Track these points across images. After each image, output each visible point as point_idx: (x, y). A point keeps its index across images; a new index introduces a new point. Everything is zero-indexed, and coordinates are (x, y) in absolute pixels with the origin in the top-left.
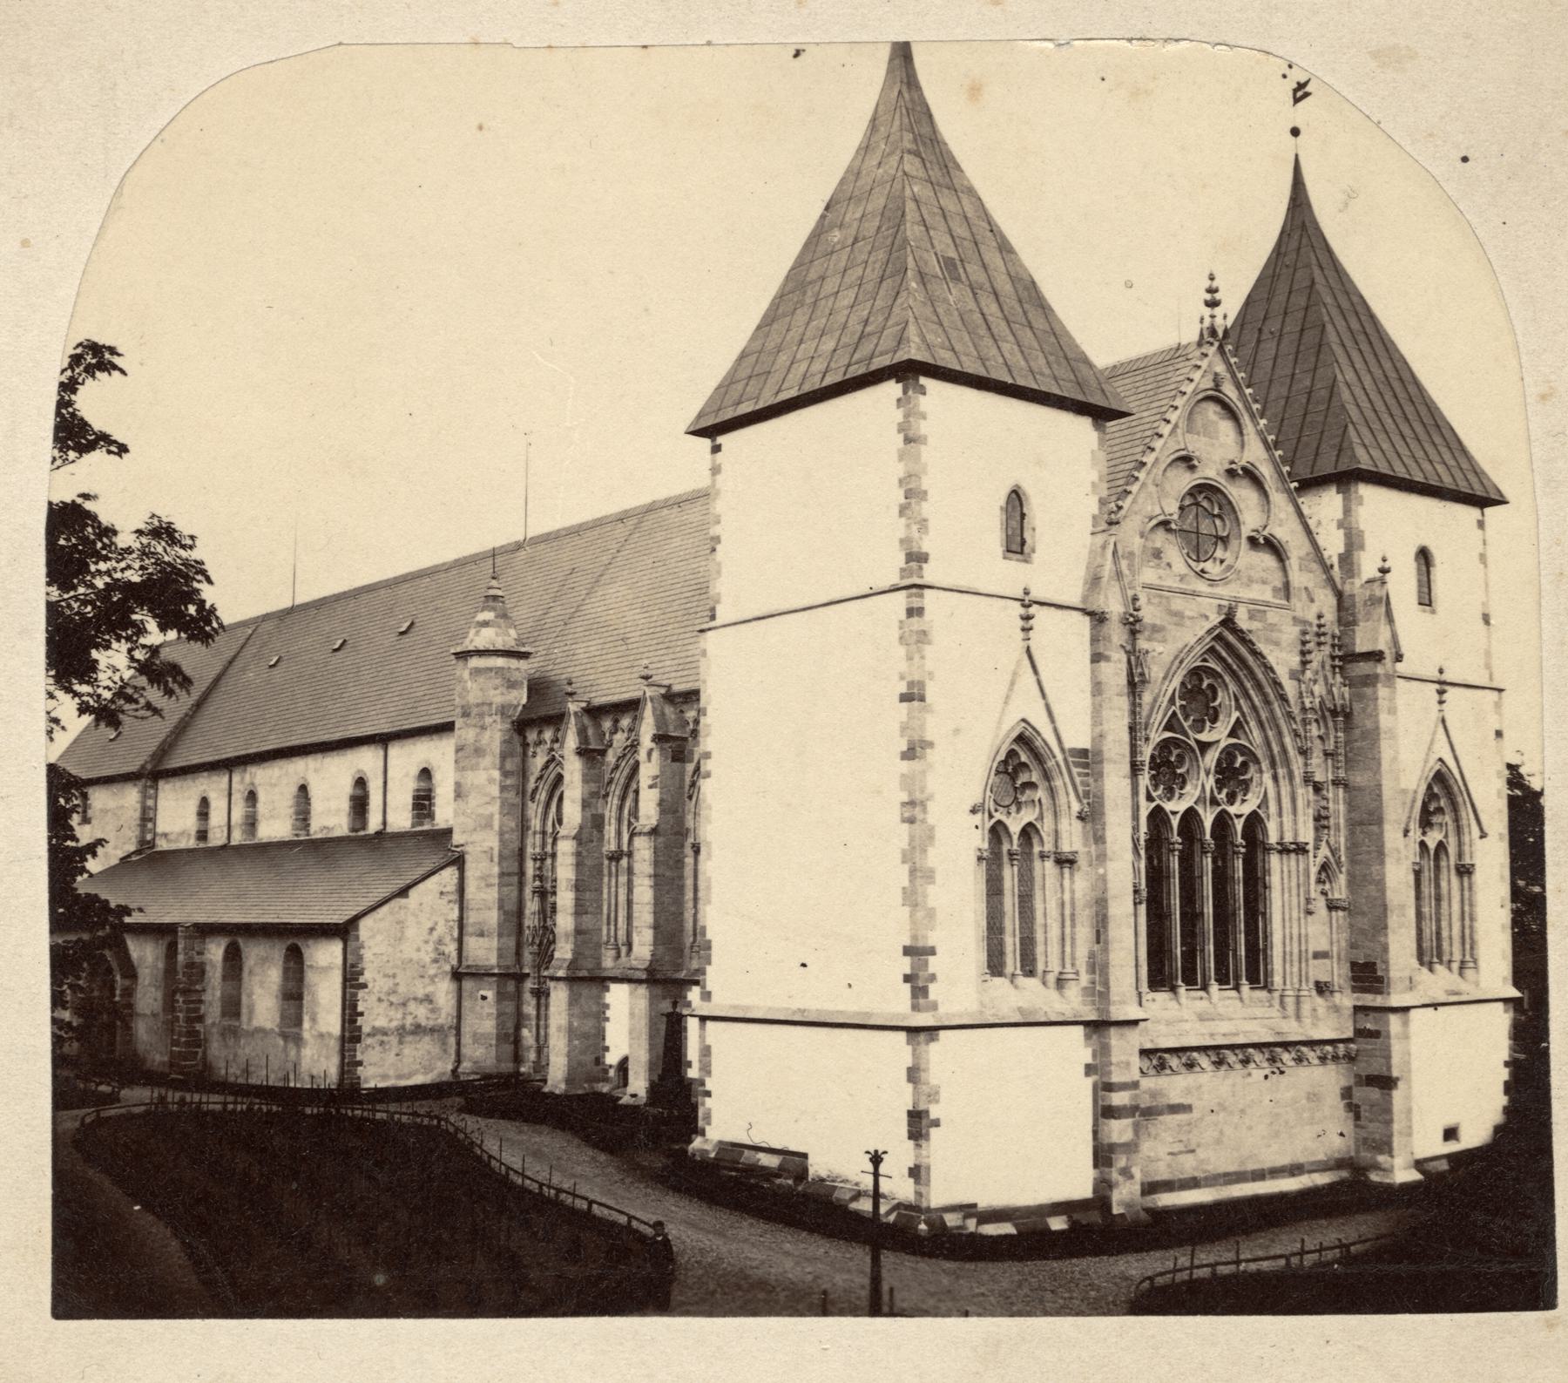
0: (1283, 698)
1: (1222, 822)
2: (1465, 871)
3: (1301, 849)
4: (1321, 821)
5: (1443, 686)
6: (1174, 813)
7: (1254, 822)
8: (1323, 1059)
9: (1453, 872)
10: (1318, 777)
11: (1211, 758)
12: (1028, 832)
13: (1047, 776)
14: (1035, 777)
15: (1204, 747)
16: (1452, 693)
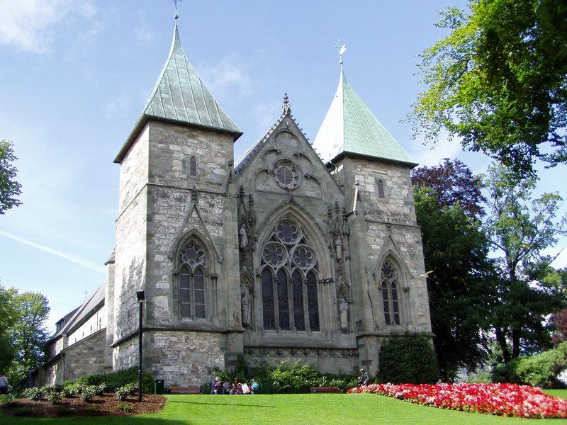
0: (320, 229)
1: (297, 272)
2: (407, 290)
3: (331, 281)
4: (340, 271)
5: (389, 225)
6: (275, 269)
7: (312, 274)
8: (344, 355)
9: (402, 291)
10: (339, 255)
11: (293, 250)
12: (199, 269)
13: (207, 250)
14: (202, 250)
15: (290, 247)
16: (392, 227)
